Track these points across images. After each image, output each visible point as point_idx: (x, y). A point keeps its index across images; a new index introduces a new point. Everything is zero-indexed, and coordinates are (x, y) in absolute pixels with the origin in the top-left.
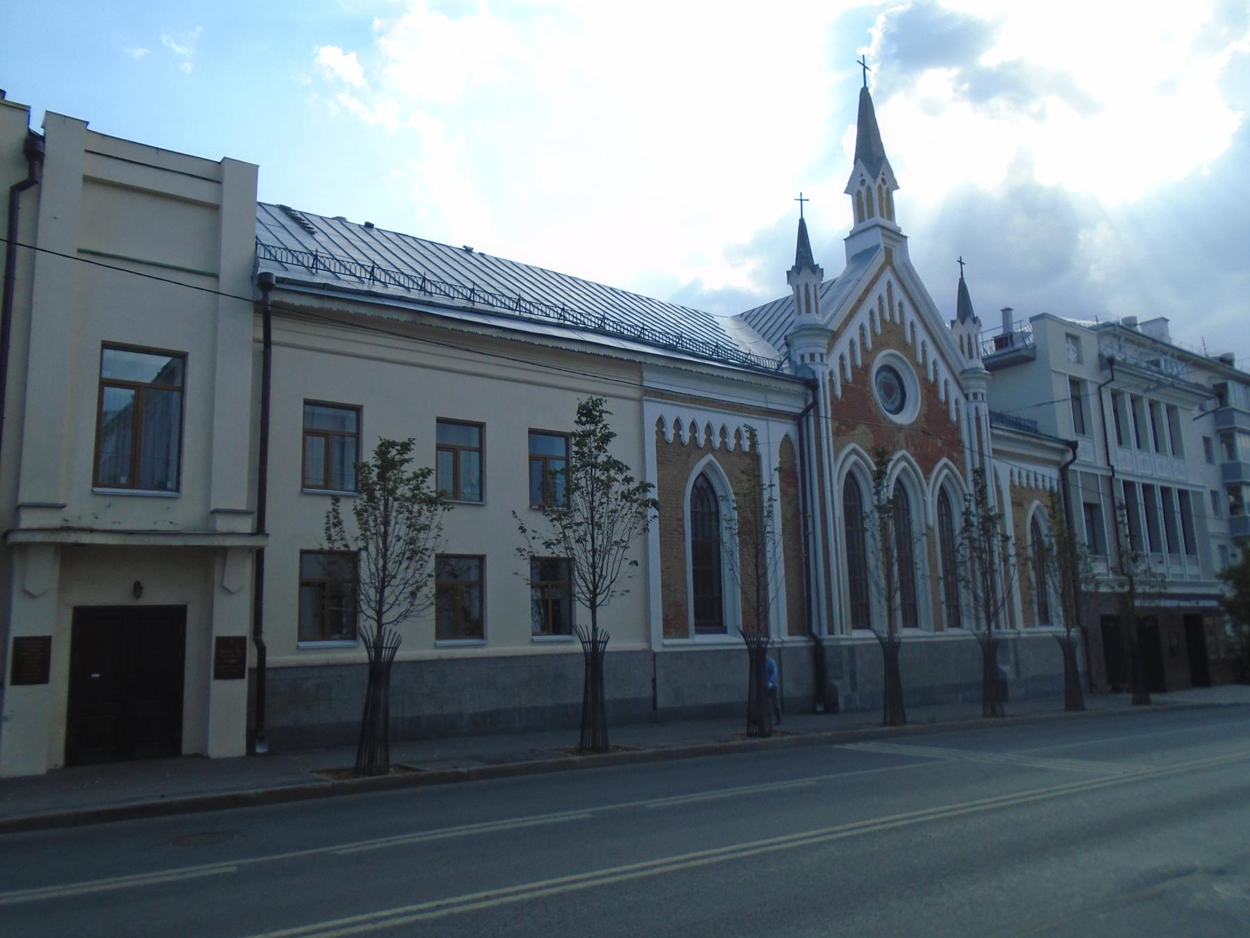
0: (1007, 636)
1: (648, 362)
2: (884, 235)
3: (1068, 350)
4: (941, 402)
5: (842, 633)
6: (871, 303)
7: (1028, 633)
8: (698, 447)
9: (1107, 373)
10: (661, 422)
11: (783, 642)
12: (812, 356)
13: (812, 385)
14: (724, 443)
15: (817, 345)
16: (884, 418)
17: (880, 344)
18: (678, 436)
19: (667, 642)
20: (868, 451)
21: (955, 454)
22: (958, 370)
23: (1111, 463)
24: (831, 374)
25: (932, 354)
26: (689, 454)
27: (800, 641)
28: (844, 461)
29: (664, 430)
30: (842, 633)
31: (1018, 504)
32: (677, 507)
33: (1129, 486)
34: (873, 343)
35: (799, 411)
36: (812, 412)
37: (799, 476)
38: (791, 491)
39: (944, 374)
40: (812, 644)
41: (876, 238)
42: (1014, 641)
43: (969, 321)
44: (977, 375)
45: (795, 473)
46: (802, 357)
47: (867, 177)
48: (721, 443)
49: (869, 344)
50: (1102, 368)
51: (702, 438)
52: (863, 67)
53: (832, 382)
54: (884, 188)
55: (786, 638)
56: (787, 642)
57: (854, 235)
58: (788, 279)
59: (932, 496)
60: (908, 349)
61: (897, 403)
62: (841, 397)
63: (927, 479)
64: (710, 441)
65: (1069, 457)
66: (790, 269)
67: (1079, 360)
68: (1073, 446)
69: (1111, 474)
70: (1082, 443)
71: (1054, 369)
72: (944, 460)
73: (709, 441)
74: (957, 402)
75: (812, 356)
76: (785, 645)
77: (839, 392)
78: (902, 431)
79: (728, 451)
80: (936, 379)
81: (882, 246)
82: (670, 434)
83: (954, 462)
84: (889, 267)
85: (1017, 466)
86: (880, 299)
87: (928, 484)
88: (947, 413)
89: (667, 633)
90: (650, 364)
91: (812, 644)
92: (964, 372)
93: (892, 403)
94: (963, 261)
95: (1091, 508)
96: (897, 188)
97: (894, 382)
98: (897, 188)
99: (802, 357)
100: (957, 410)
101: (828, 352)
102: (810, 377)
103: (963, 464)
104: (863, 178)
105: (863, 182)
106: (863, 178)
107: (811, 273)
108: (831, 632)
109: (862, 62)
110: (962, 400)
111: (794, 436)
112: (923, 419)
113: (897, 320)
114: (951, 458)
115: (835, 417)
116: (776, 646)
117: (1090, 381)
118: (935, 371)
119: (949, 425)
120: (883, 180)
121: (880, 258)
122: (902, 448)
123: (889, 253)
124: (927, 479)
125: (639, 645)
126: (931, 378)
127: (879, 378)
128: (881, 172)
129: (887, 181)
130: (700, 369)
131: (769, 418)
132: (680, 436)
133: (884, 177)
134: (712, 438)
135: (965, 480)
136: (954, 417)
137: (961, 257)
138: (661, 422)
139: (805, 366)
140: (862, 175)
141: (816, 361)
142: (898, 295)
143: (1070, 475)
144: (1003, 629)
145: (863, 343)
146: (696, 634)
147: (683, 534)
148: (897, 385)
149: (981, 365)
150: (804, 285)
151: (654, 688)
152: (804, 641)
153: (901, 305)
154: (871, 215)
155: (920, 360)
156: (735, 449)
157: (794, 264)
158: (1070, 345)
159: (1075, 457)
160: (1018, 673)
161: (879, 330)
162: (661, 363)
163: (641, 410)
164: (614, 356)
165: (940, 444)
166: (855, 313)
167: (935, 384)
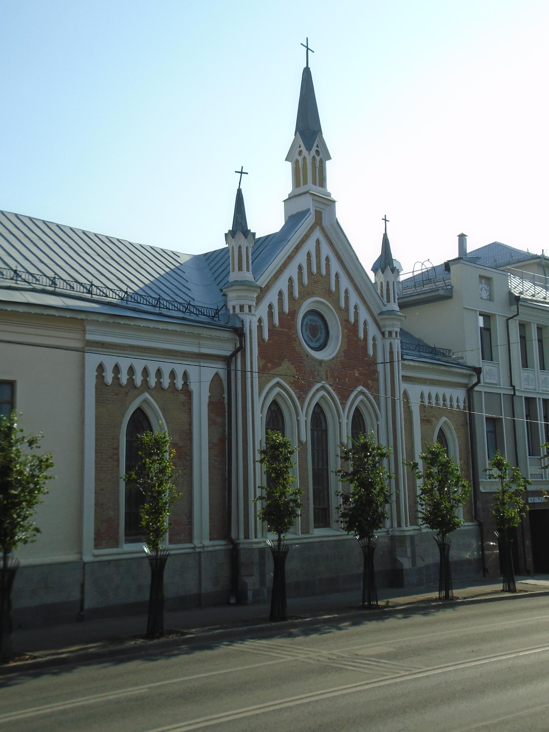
0: (407, 533)
1: (89, 319)
2: (313, 199)
3: (481, 289)
4: (360, 340)
5: (256, 537)
6: (301, 258)
8: (135, 387)
9: (514, 308)
10: (101, 368)
11: (203, 547)
12: (242, 308)
13: (239, 332)
14: (159, 383)
15: (245, 298)
16: (307, 356)
17: (306, 293)
18: (116, 379)
19: (97, 552)
20: (291, 384)
21: (370, 382)
22: (376, 312)
23: (513, 384)
24: (260, 321)
25: (354, 299)
26: (127, 393)
27: (220, 545)
28: (268, 393)
29: (104, 374)
30: (256, 537)
31: (426, 421)
32: (113, 439)
33: (530, 401)
34: (300, 293)
35: (228, 353)
36: (239, 354)
37: (226, 406)
38: (219, 420)
39: (364, 315)
40: (231, 547)
41: (306, 203)
42: (412, 537)
43: (388, 270)
44: (392, 317)
45: (223, 403)
46: (234, 308)
47: (303, 148)
48: (156, 382)
49: (296, 294)
50: (511, 305)
51: (138, 380)
52: (306, 49)
53: (260, 328)
54: (318, 158)
55: (207, 542)
56: (208, 547)
57: (291, 197)
58: (226, 240)
59: (347, 419)
60: (333, 296)
61: (322, 341)
62: (269, 339)
63: (343, 404)
64: (147, 381)
65: (475, 380)
66: (227, 232)
67: (490, 298)
68: (478, 371)
69: (513, 393)
70: (486, 367)
71: (465, 307)
72: (360, 388)
73: (145, 382)
74: (374, 339)
75: (242, 308)
76: (206, 549)
78: (323, 364)
79: (163, 389)
80: (356, 320)
81: (312, 211)
82: (109, 377)
83: (369, 390)
84: (318, 227)
85: (426, 389)
86: (309, 255)
87: (344, 409)
88: (365, 347)
89: (97, 546)
90: (92, 320)
91: (231, 547)
92: (381, 313)
93: (316, 341)
94: (387, 219)
95: (494, 423)
96: (329, 158)
97: (320, 323)
98: (329, 158)
99: (234, 308)
100: (375, 346)
101: (257, 304)
102: (239, 325)
103: (378, 391)
104: (300, 149)
105: (300, 153)
106: (300, 149)
107: (243, 236)
108: (247, 537)
109: (306, 45)
110: (379, 336)
111: (223, 374)
112: (343, 354)
113: (324, 271)
114: (366, 386)
115: (261, 355)
116: (198, 550)
117: (498, 315)
118: (356, 314)
119: (366, 359)
120: (317, 152)
121: (310, 220)
123: (319, 215)
124: (343, 404)
125: (72, 557)
126: (352, 320)
127: (305, 323)
128: (315, 145)
129: (321, 152)
131: (201, 360)
132: (118, 379)
133: (319, 149)
134: (148, 379)
135: (379, 405)
136: (371, 352)
137: (385, 216)
138: (101, 368)
139: (235, 315)
140: (300, 147)
142: (326, 250)
143: (475, 396)
144: (404, 528)
145: (291, 293)
146: (125, 543)
147: (118, 460)
148: (323, 327)
149: (396, 308)
150: (238, 246)
151: (82, 592)
152: (225, 545)
153: (327, 259)
154: (305, 182)
155: (343, 305)
156: (169, 387)
157: (231, 229)
158: (484, 286)
159: (479, 382)
160: (414, 563)
161: (306, 281)
162: (101, 319)
163: (83, 358)
164: (57, 315)
165: (357, 375)
166: (285, 269)
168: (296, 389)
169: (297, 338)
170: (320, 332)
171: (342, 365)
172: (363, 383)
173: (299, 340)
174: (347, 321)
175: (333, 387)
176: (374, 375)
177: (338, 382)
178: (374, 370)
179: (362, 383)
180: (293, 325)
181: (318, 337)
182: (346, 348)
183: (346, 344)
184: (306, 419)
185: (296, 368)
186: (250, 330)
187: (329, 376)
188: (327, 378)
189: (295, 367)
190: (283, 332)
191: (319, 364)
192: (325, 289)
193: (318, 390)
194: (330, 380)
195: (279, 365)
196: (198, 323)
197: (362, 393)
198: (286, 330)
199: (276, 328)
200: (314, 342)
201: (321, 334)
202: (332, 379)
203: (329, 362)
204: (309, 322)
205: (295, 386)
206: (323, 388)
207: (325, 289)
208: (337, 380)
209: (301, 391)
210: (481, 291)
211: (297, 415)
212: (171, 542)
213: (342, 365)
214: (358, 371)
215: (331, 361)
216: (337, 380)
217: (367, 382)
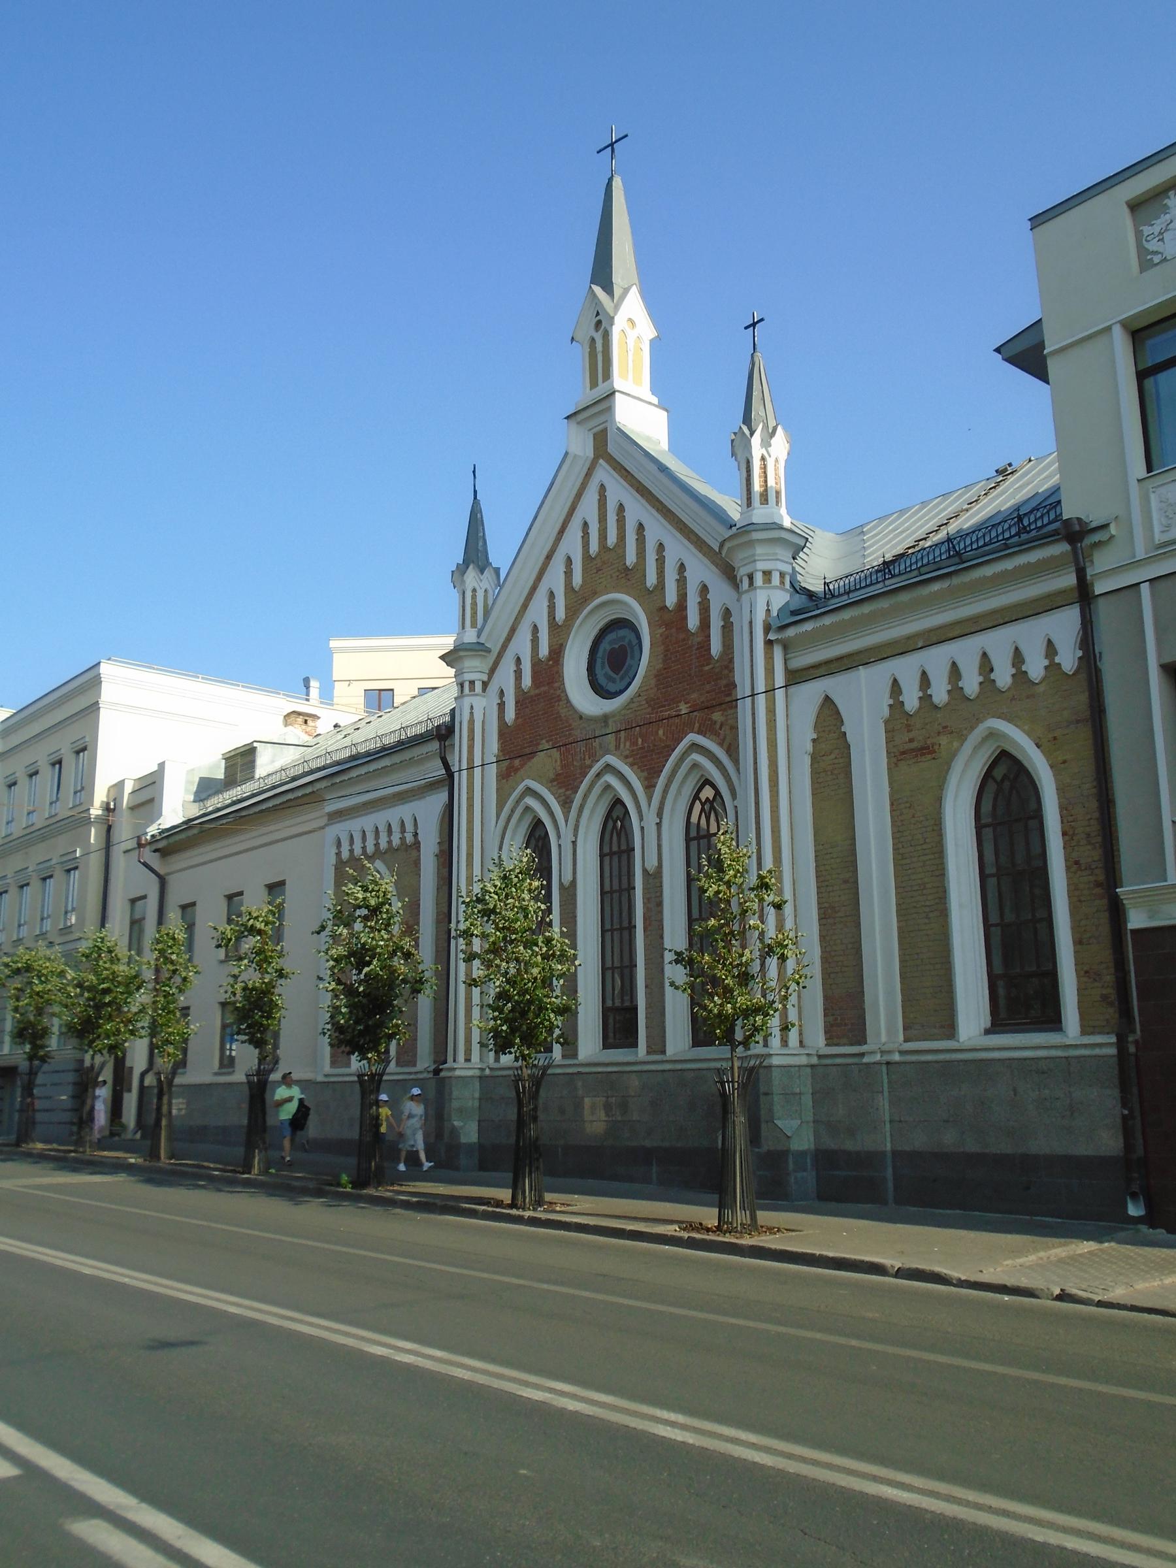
2: (578, 423)
5: (454, 1061)
7: (901, 1053)
10: (339, 844)
16: (581, 718)
49: (560, 614)
53: (501, 706)
77: (510, 715)
78: (610, 722)
93: (622, 679)
112: (653, 682)
113: (612, 539)
119: (707, 668)
122: (608, 752)
126: (671, 599)
127: (600, 654)
130: (354, 774)
138: (339, 844)
167: (682, 605)
168: (560, 788)
169: (562, 695)
170: (629, 655)
172: (700, 727)
174: (664, 608)
175: (631, 760)
177: (642, 744)
178: (726, 686)
179: (697, 725)
180: (557, 672)
181: (627, 664)
183: (662, 656)
187: (622, 740)
188: (617, 747)
190: (540, 694)
191: (603, 724)
192: (618, 571)
193: (598, 775)
194: (625, 745)
198: (546, 688)
199: (529, 694)
200: (618, 682)
201: (632, 657)
202: (628, 744)
203: (623, 712)
204: (627, 640)
205: (558, 784)
207: (618, 571)
208: (640, 741)
209: (567, 790)
210: (1162, 240)
212: (398, 1064)
213: (650, 706)
215: (627, 707)
216: (640, 741)
217: (710, 719)
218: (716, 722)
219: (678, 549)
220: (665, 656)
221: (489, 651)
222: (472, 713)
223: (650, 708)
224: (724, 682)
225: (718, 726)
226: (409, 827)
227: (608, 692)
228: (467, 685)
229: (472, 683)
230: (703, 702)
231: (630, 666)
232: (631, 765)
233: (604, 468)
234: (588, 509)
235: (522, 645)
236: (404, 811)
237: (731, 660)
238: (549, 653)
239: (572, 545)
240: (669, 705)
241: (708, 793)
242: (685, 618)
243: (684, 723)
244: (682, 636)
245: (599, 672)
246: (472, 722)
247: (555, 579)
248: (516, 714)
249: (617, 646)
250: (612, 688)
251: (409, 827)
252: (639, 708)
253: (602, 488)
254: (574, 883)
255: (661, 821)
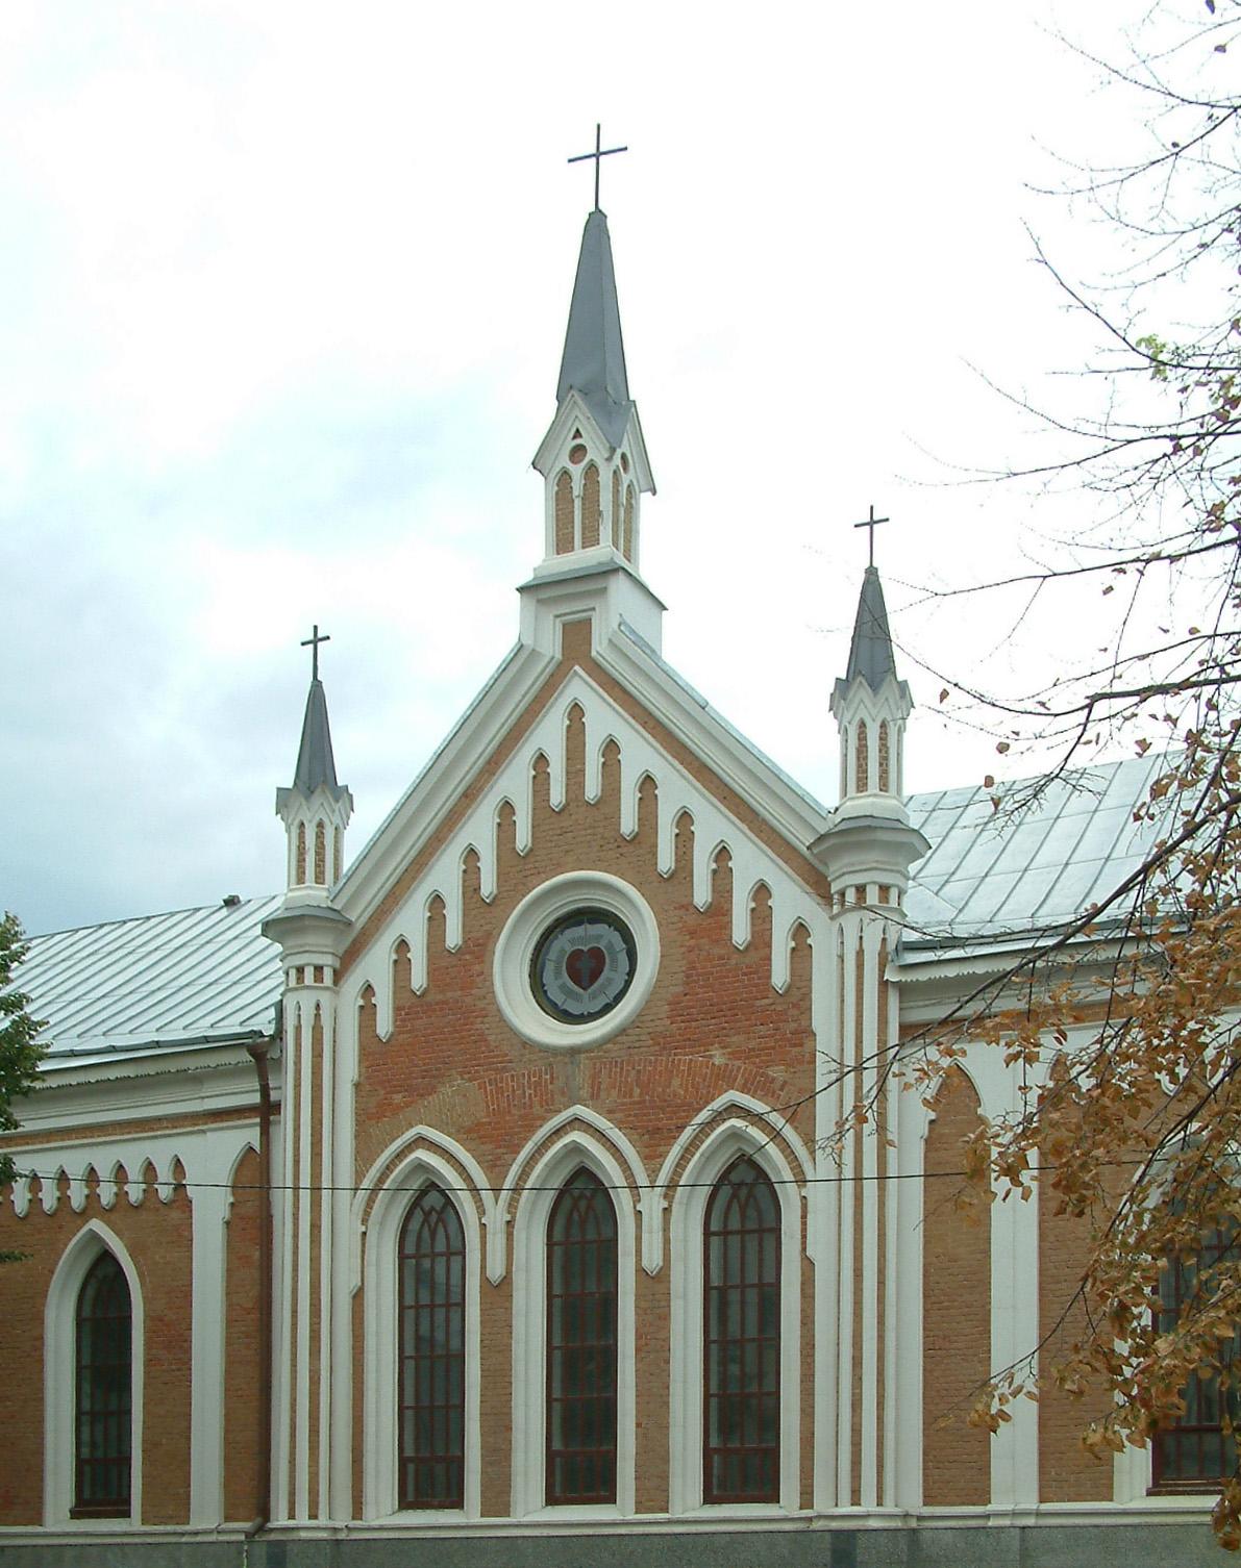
14: (121, 1195)
20: (465, 1134)
21: (777, 1072)
22: (802, 839)
34: (502, 876)
49: (488, 886)
51: (77, 1195)
53: (367, 1011)
73: (92, 1198)
77: (384, 1025)
93: (594, 997)
100: (801, 952)
113: (592, 789)
126: (702, 895)
127: (553, 954)
136: (780, 975)
141: (307, 983)
155: (666, 861)
167: (720, 908)
170: (607, 961)
171: (659, 1044)
172: (745, 1085)
173: (499, 1010)
174: (688, 906)
175: (619, 1115)
176: (795, 1045)
177: (641, 1095)
182: (682, 989)
184: (508, 1217)
185: (486, 1091)
186: (298, 1028)
189: (482, 1086)
190: (443, 1002)
192: (603, 838)
193: (558, 1132)
195: (433, 1090)
196: (127, 1051)
197: (734, 1109)
201: (614, 969)
202: (614, 1093)
206: (577, 1122)
207: (603, 838)
208: (637, 1091)
211: (481, 1211)
214: (723, 1048)
218: (774, 1079)
219: (713, 826)
220: (687, 977)
221: (349, 924)
222: (317, 1016)
223: (657, 1048)
224: (793, 1025)
225: (777, 1085)
226: (164, 1173)
227: (570, 1014)
228: (309, 973)
229: (319, 969)
230: (753, 1049)
231: (610, 981)
232: (620, 1125)
233: (580, 677)
234: (549, 736)
235: (411, 921)
236: (161, 1151)
237: (807, 996)
238: (465, 942)
239: (515, 782)
240: (691, 1047)
241: (743, 1174)
242: (728, 925)
243: (718, 1075)
244: (717, 951)
245: (548, 977)
246: (317, 1030)
247: (480, 830)
248: (396, 1027)
249: (585, 949)
250: (574, 1008)
251: (164, 1173)
252: (637, 1045)
253: (576, 711)
254: (507, 1279)
255: (670, 1206)
